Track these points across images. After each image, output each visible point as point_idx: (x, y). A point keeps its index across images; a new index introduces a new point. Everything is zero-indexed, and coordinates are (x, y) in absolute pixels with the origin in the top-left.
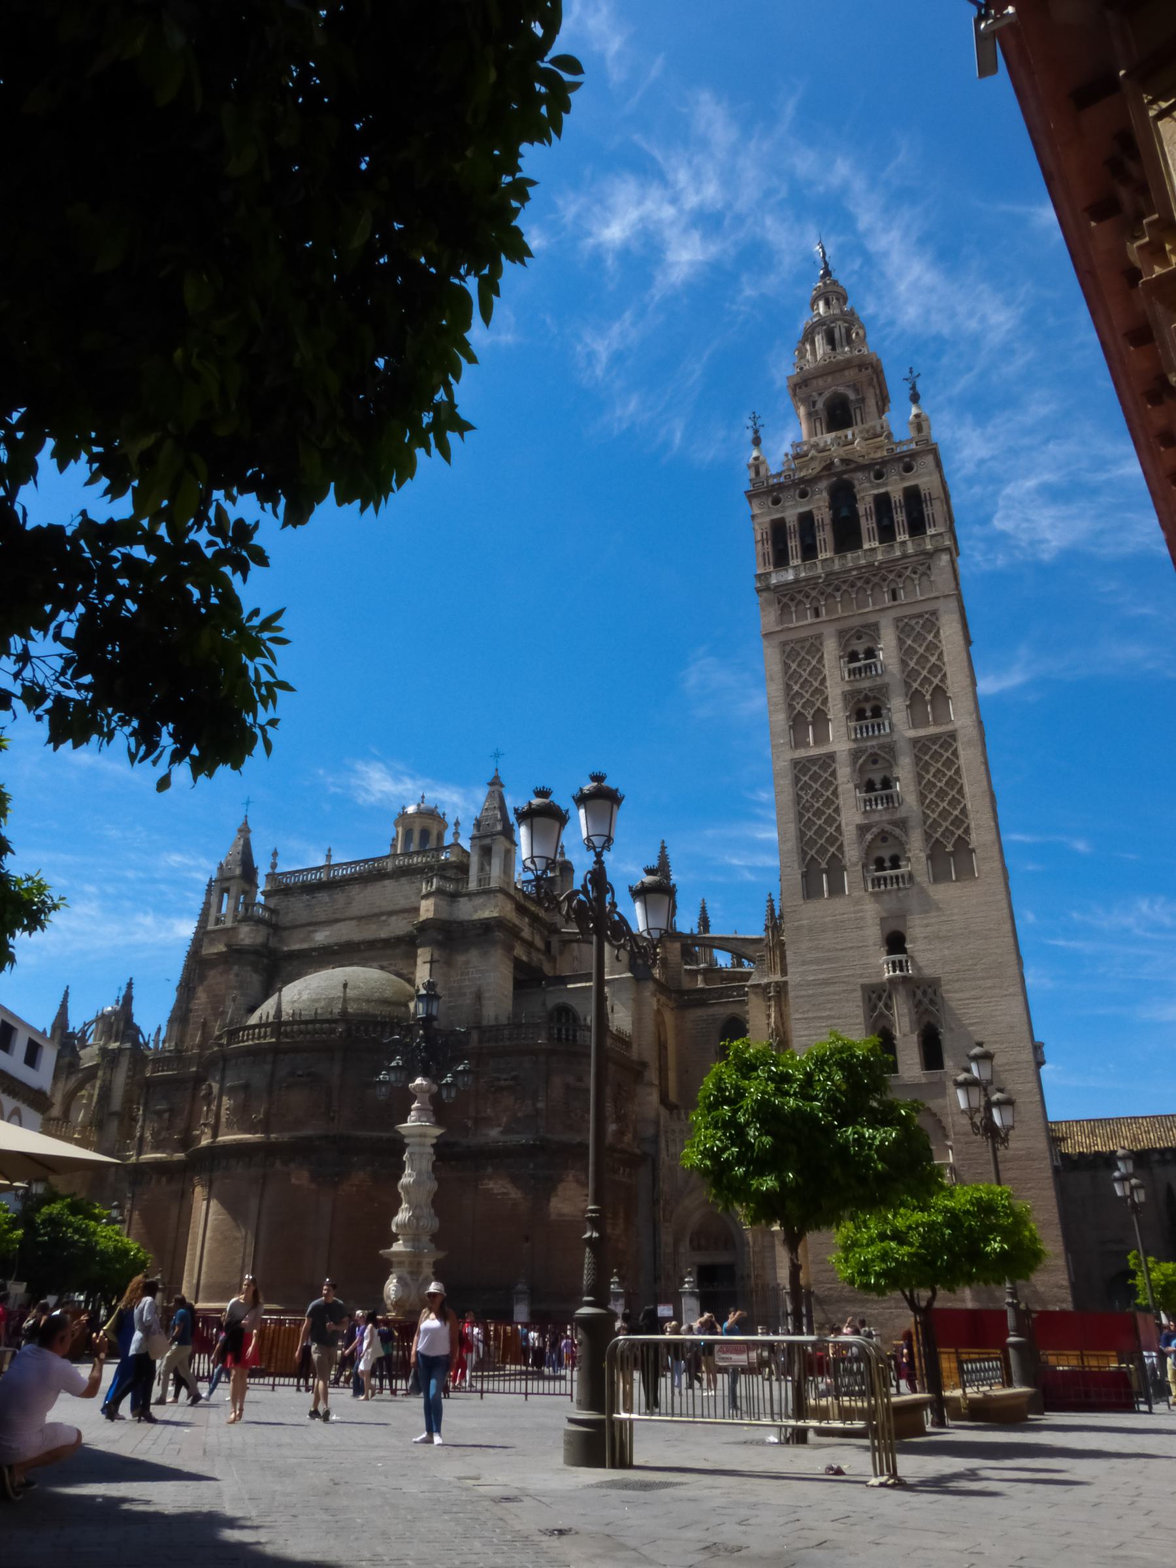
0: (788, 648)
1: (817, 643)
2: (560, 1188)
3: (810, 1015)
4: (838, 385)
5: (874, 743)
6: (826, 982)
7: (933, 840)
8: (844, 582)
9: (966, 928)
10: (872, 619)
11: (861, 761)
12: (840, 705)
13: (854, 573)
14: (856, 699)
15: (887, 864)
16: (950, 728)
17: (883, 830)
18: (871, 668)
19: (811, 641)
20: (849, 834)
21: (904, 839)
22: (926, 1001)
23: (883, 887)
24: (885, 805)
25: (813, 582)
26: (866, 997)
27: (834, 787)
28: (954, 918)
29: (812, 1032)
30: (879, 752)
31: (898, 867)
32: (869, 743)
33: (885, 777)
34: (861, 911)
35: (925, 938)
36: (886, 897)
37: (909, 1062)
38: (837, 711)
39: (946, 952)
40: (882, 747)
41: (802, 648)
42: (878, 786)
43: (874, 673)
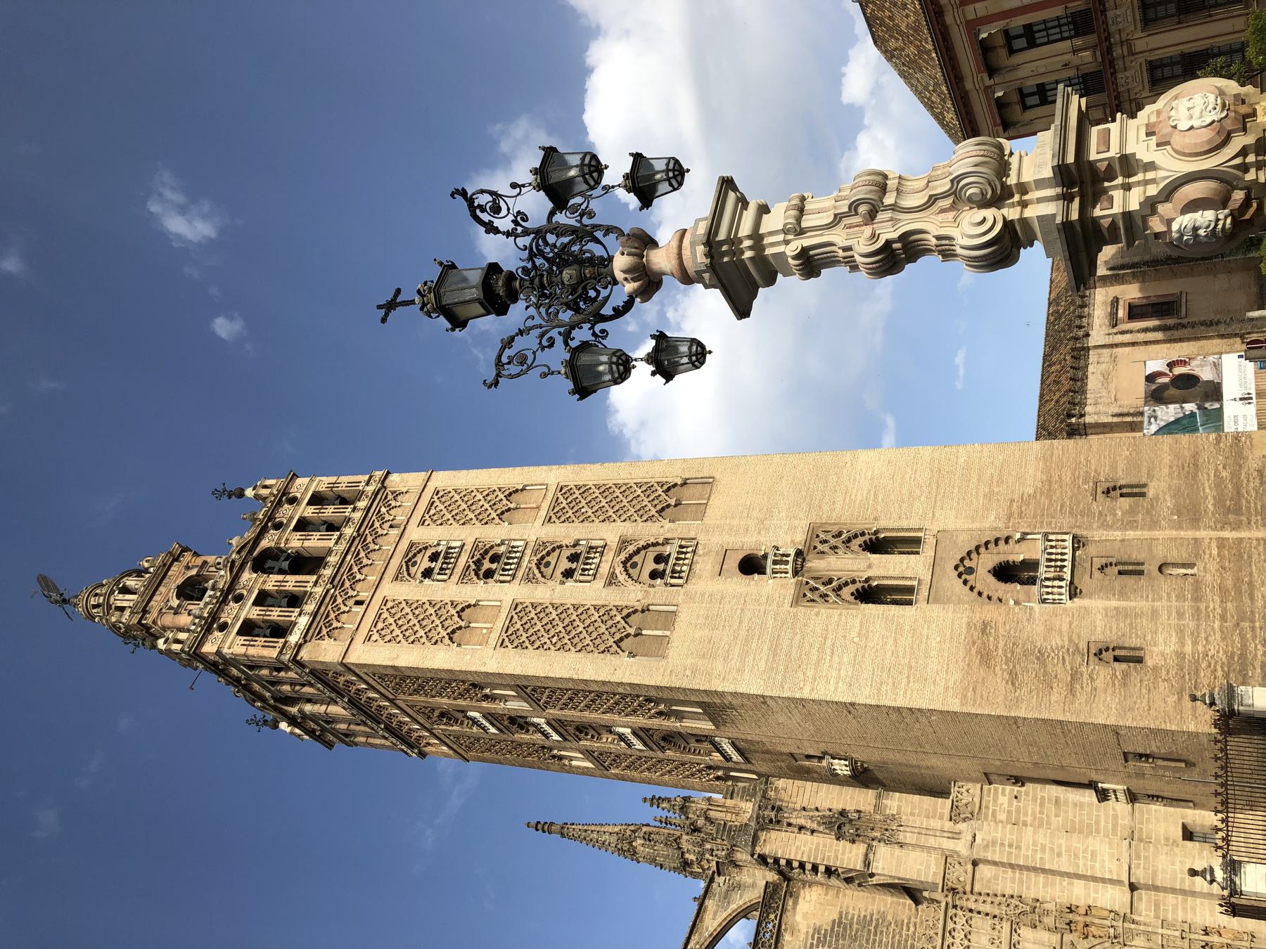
1: (390, 604)
3: (810, 673)
6: (775, 650)
7: (657, 515)
9: (764, 494)
10: (404, 545)
12: (469, 587)
14: (473, 573)
15: (661, 567)
16: (552, 489)
17: (624, 563)
20: (612, 597)
21: (642, 543)
22: (833, 542)
23: (684, 568)
24: (598, 554)
26: (809, 604)
28: (748, 503)
29: (835, 673)
30: (539, 556)
31: (669, 555)
32: (524, 564)
33: (568, 558)
34: (703, 595)
35: (759, 533)
36: (697, 568)
37: (905, 566)
38: (476, 591)
39: (783, 514)
40: (535, 552)
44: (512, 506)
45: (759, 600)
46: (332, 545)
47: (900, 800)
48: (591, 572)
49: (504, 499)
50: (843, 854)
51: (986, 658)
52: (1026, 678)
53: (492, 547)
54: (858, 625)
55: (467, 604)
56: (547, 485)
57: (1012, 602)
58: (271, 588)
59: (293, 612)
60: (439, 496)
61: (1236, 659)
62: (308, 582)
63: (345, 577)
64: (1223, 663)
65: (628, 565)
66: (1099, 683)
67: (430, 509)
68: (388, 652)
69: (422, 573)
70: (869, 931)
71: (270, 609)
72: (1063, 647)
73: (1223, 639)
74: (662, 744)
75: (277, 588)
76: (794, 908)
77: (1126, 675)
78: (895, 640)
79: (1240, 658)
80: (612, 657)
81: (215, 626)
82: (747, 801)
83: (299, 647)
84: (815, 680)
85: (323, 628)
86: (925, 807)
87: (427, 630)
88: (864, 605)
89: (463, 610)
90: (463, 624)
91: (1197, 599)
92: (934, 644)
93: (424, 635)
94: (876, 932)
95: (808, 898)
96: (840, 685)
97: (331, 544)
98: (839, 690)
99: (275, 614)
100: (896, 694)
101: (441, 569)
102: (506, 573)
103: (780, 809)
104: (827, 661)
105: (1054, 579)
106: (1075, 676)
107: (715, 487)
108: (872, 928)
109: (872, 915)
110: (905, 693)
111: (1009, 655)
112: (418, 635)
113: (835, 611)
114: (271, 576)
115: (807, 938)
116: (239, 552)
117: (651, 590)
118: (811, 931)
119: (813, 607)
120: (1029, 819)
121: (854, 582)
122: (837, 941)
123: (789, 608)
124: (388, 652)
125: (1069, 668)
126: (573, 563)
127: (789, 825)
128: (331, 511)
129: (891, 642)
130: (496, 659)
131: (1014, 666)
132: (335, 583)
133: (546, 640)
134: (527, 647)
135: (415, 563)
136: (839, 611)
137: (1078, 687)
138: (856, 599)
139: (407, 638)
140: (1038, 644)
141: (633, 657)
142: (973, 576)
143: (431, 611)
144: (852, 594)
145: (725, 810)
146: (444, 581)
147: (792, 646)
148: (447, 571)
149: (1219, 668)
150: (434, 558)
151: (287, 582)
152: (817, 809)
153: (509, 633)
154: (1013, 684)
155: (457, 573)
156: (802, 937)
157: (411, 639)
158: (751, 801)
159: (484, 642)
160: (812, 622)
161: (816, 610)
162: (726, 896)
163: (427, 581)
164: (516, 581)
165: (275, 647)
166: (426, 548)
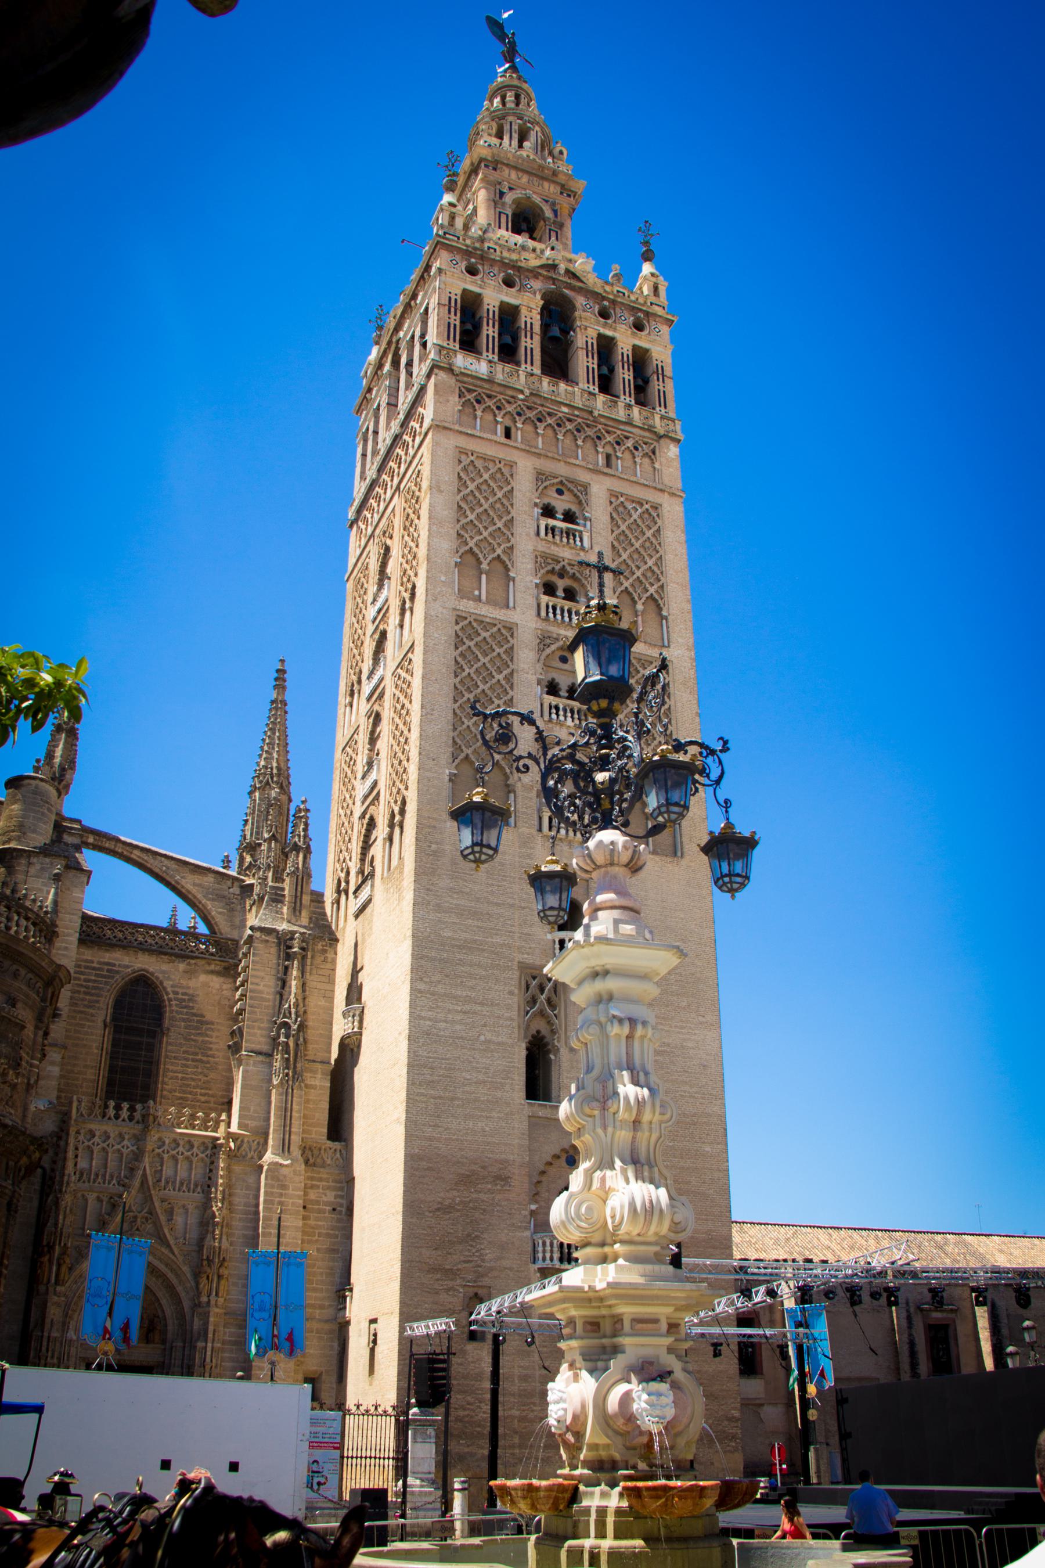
0: (466, 461)
1: (506, 471)
3: (440, 989)
4: (534, 192)
8: (550, 414)
10: (583, 476)
11: (548, 651)
12: (530, 566)
14: (549, 568)
18: (574, 536)
19: (499, 466)
24: (577, 722)
25: (510, 393)
26: (523, 983)
27: (509, 671)
29: (441, 1016)
41: (487, 469)
42: (564, 693)
43: (578, 543)
44: (640, 607)
45: (525, 924)
46: (581, 385)
47: (322, 1087)
48: (554, 716)
49: (648, 594)
50: (260, 1028)
51: (467, 1180)
52: (446, 1223)
53: (583, 585)
54: (500, 1039)
55: (510, 566)
56: (669, 646)
57: (533, 1207)
58: (523, 319)
59: (493, 353)
60: (651, 510)
61: (478, 1429)
62: (532, 364)
63: (540, 409)
64: (472, 1417)
66: (443, 1297)
67: (633, 501)
68: (447, 479)
69: (549, 504)
70: (197, 1054)
71: (497, 324)
72: (483, 1261)
74: (368, 816)
75: (523, 326)
76: (212, 972)
78: (484, 1082)
79: (478, 1433)
80: (449, 754)
81: (473, 260)
82: (310, 918)
83: (450, 370)
84: (433, 994)
85: (475, 394)
86: (317, 1115)
87: (476, 522)
88: (524, 1045)
89: (503, 563)
90: (485, 566)
92: (480, 1124)
93: (468, 519)
94: (197, 1061)
95: (225, 986)
96: (428, 1023)
97: (583, 385)
98: (422, 1022)
99: (490, 331)
100: (420, 1085)
101: (553, 529)
102: (551, 610)
103: (304, 957)
104: (456, 1007)
105: (562, 1253)
106: (451, 1273)
107: (669, 859)
108: (199, 1057)
109: (213, 1056)
110: (422, 1095)
111: (471, 1205)
112: (468, 512)
113: (516, 1013)
114: (539, 317)
115: (183, 988)
116: (568, 272)
118: (191, 992)
119: (520, 982)
120: (312, 1222)
121: (553, 1032)
122: (183, 1020)
123: (517, 959)
124: (447, 479)
125: (460, 1266)
126: (568, 691)
127: (286, 968)
128: (626, 377)
129: (481, 1077)
130: (442, 613)
131: (458, 1211)
132: (534, 399)
133: (467, 671)
134: (457, 648)
135: (560, 492)
136: (515, 1017)
137: (439, 1276)
138: (533, 1036)
139: (464, 499)
140: (485, 1236)
141: (450, 780)
142: (564, 1164)
143: (500, 524)
144: (538, 1032)
145: (299, 894)
146: (538, 534)
147: (471, 966)
148: (550, 535)
149: (466, 1413)
150: (569, 517)
151: (532, 338)
152: (304, 999)
153: (475, 624)
154: (438, 1209)
155: (549, 548)
156: (184, 982)
157: (463, 505)
158: (310, 923)
159: (463, 594)
160: (501, 988)
161: (516, 991)
162: (220, 897)
163: (537, 511)
164: (541, 625)
165: (448, 339)
166: (580, 503)
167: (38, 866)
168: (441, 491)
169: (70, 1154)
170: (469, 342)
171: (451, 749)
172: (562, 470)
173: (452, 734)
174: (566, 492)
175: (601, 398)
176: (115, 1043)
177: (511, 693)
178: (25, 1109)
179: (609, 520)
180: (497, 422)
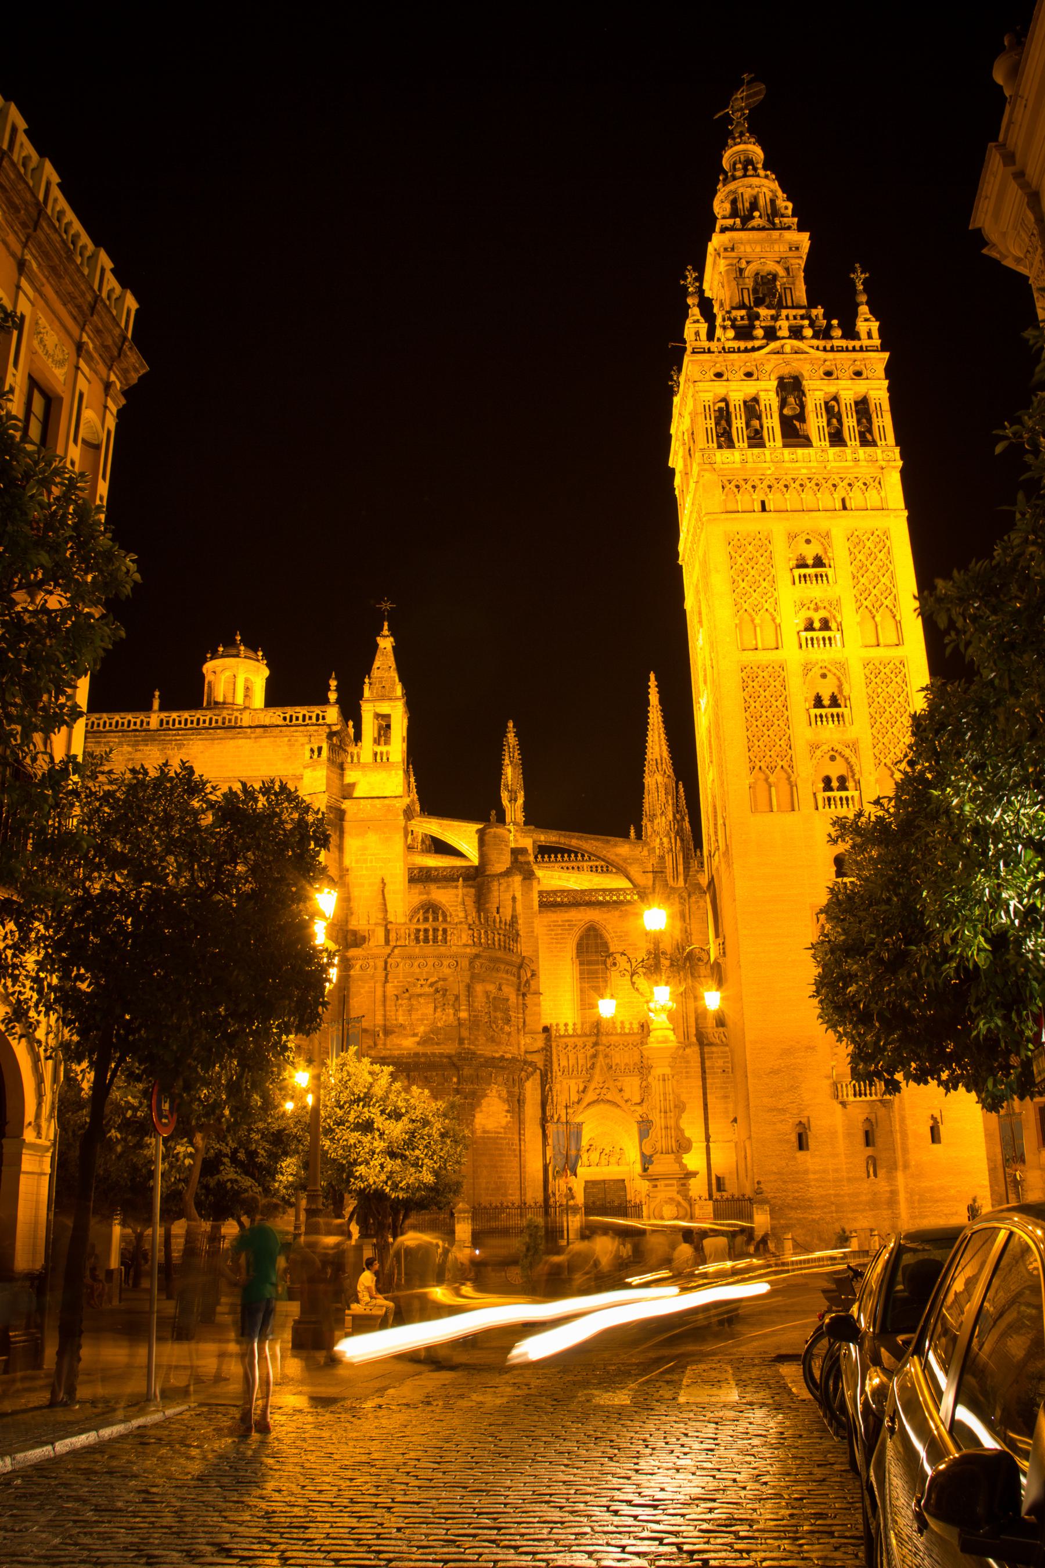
2: (484, 1102)
5: (825, 657)
13: (804, 471)
15: (835, 784)
18: (821, 576)
20: (800, 750)
23: (833, 806)
24: (836, 723)
30: (829, 666)
31: (846, 789)
42: (826, 702)
48: (819, 723)
51: (788, 1052)
57: (833, 1063)
65: (832, 753)
66: (779, 1126)
73: (822, 1196)
77: (788, 1141)
91: (849, 1180)
102: (809, 642)
106: (783, 1111)
117: (810, 783)
133: (753, 704)
135: (808, 542)
167: (505, 885)
168: (717, 571)
169: (555, 1059)
170: (725, 439)
171: (748, 765)
172: (805, 523)
173: (748, 754)
174: (812, 540)
175: (833, 451)
176: (581, 972)
177: (786, 713)
178: (519, 1044)
179: (848, 553)
180: (753, 500)
